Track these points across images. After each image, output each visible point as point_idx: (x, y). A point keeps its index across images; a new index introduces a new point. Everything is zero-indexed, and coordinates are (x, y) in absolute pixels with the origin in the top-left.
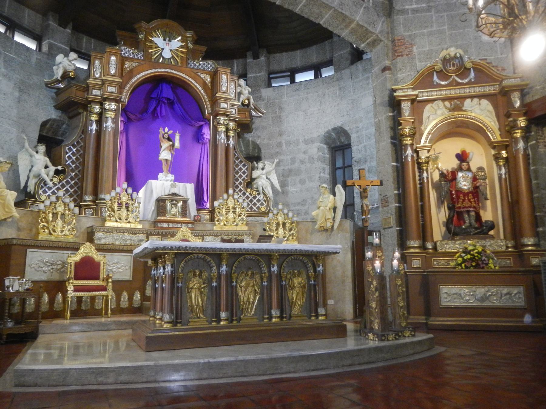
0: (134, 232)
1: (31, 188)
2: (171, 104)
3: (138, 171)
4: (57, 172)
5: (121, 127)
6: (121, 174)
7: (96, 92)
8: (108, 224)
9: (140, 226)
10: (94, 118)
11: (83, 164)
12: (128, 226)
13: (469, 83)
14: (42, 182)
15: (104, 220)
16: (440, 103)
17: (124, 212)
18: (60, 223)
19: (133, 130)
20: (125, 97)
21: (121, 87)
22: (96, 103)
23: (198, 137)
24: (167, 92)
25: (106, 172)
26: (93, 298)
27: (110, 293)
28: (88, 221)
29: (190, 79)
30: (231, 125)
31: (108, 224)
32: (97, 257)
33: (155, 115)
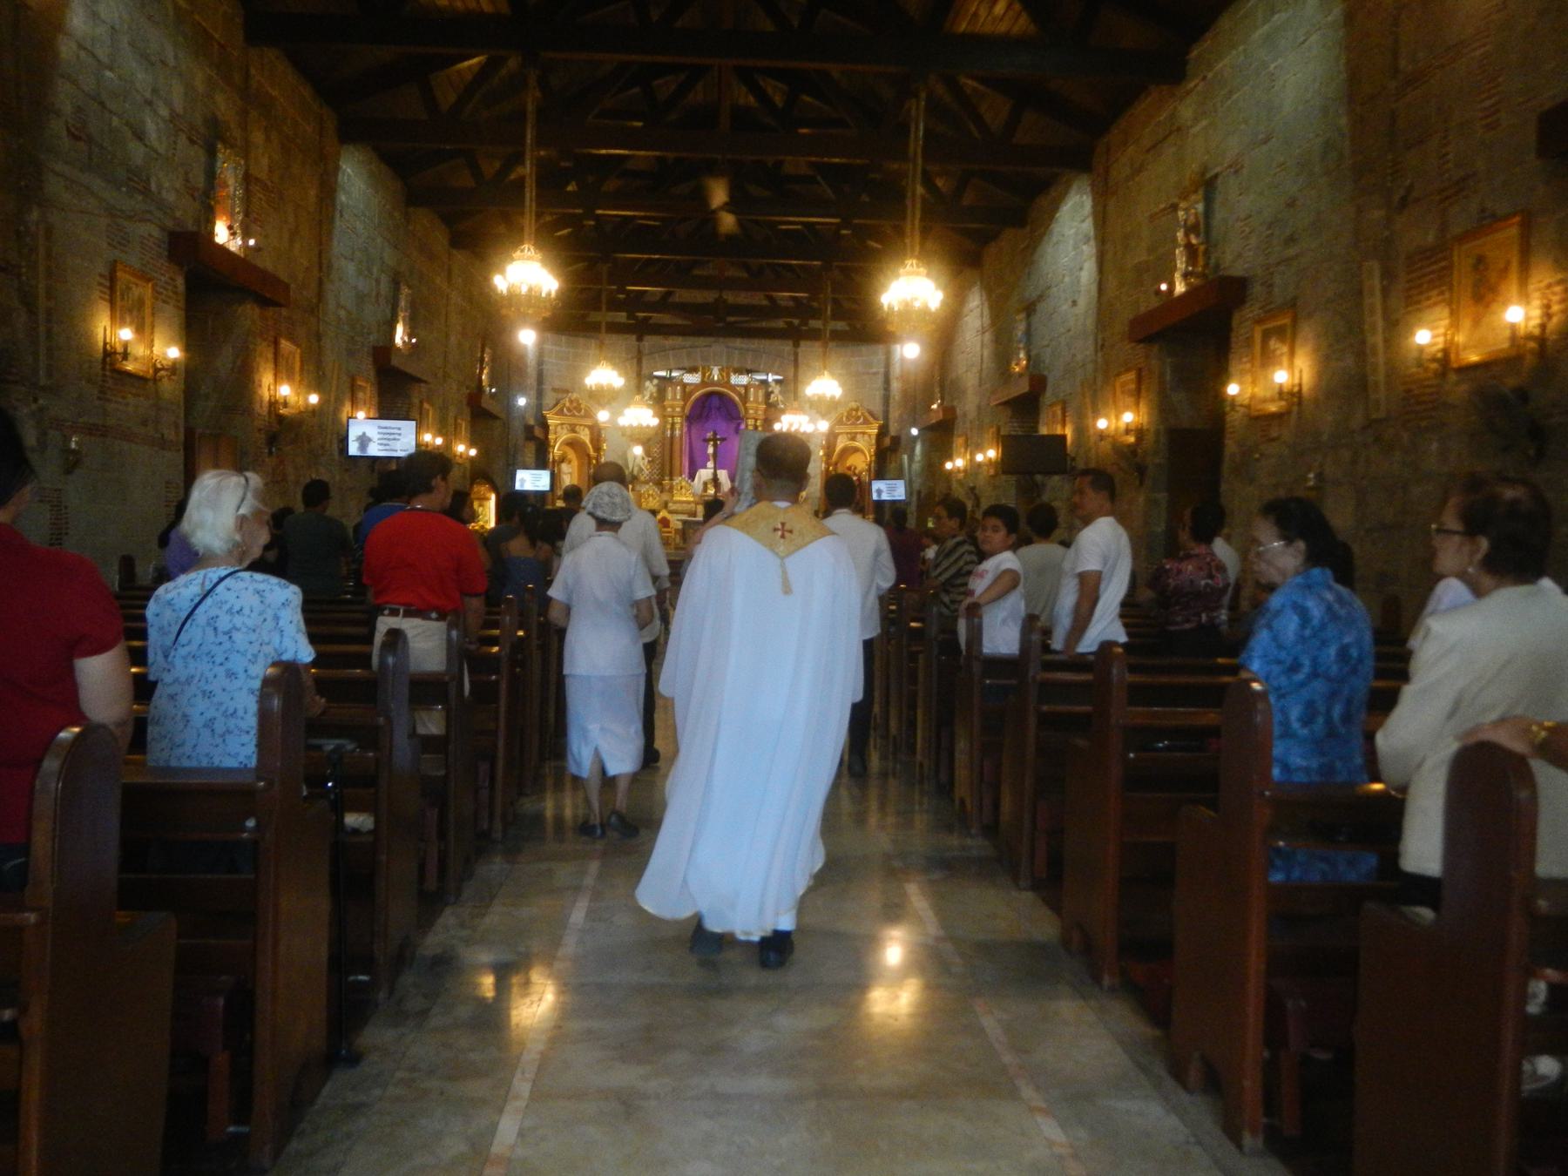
0: (689, 502)
1: (635, 473)
2: (719, 409)
3: (698, 459)
4: (649, 462)
5: (685, 429)
6: (686, 464)
7: (669, 410)
8: (675, 498)
9: (692, 499)
10: (669, 426)
11: (663, 455)
12: (685, 499)
13: (861, 424)
14: (641, 470)
15: (673, 496)
16: (845, 436)
17: (684, 490)
18: (651, 499)
19: (694, 431)
20: (687, 411)
21: (683, 408)
22: (669, 416)
23: (737, 430)
24: (715, 402)
25: (677, 463)
26: (668, 537)
27: (672, 535)
28: (665, 497)
29: (729, 392)
30: (759, 423)
31: (674, 499)
32: (669, 516)
33: (707, 417)
